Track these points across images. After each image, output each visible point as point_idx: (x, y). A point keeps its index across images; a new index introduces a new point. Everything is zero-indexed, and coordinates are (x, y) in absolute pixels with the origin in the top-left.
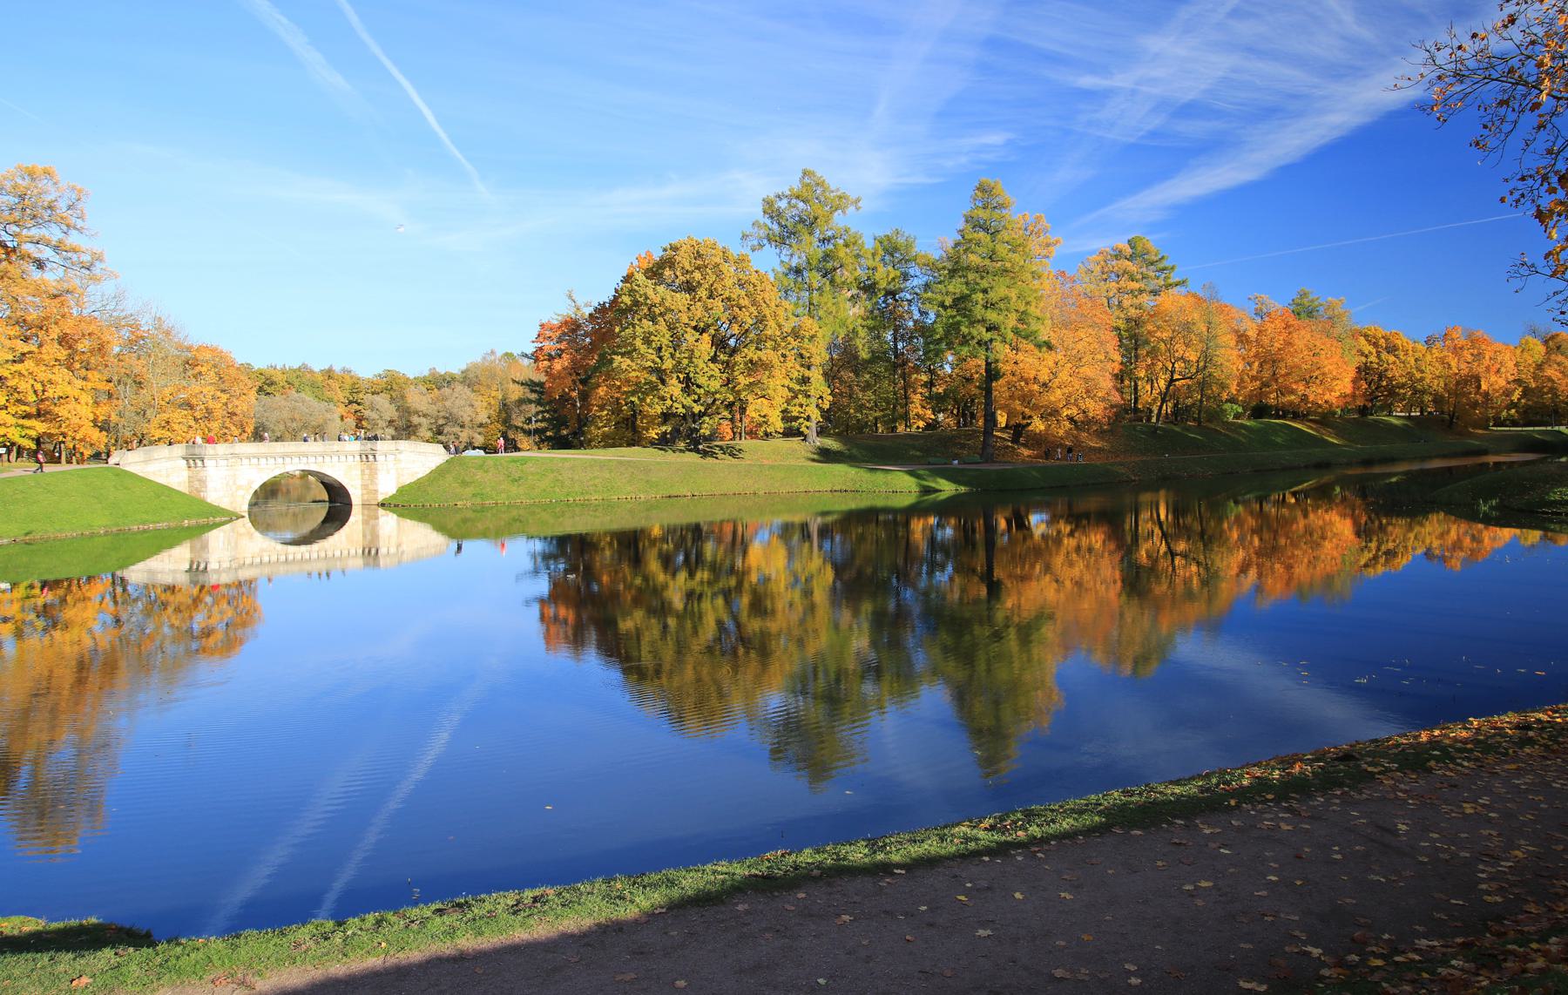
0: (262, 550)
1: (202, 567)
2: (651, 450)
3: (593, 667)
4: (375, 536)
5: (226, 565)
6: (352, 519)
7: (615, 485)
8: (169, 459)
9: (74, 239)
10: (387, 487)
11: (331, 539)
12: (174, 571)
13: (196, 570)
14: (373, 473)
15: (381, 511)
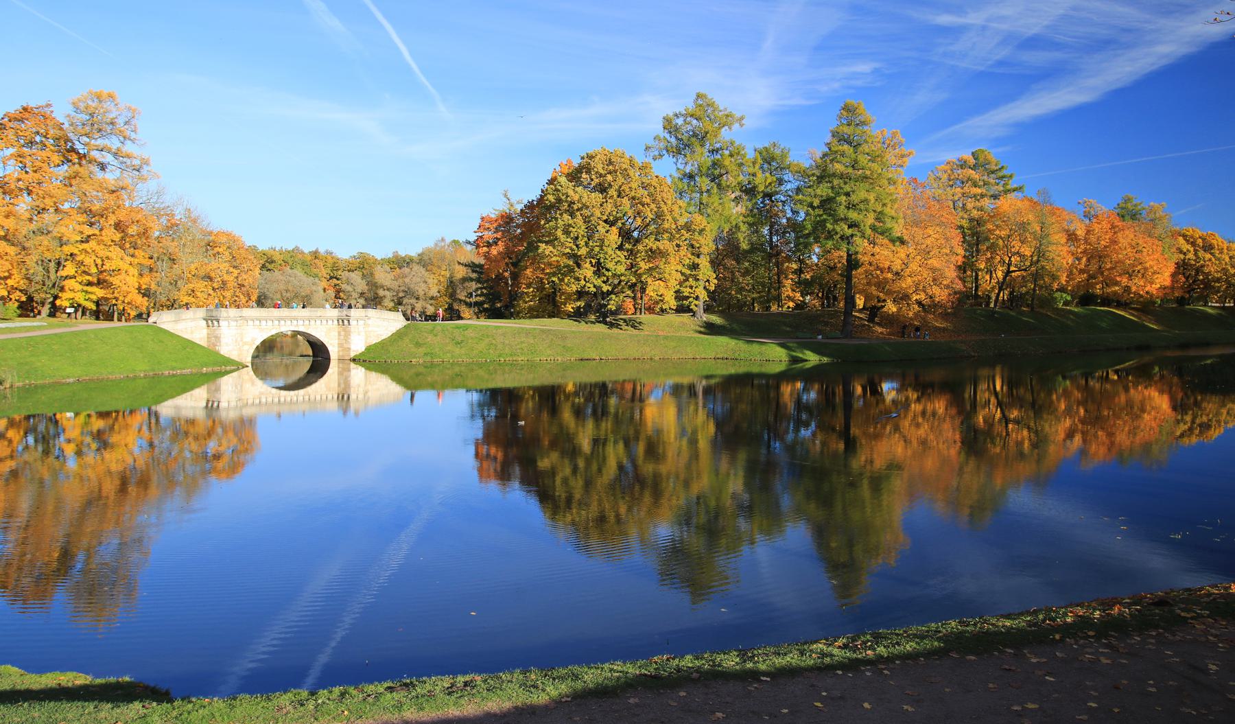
2: (567, 321)
3: (518, 496)
5: (233, 404)
6: (330, 370)
7: (538, 348)
8: (194, 319)
9: (129, 148)
10: (358, 346)
11: (314, 386)
12: (195, 408)
13: (211, 408)
14: (347, 334)
15: (352, 365)
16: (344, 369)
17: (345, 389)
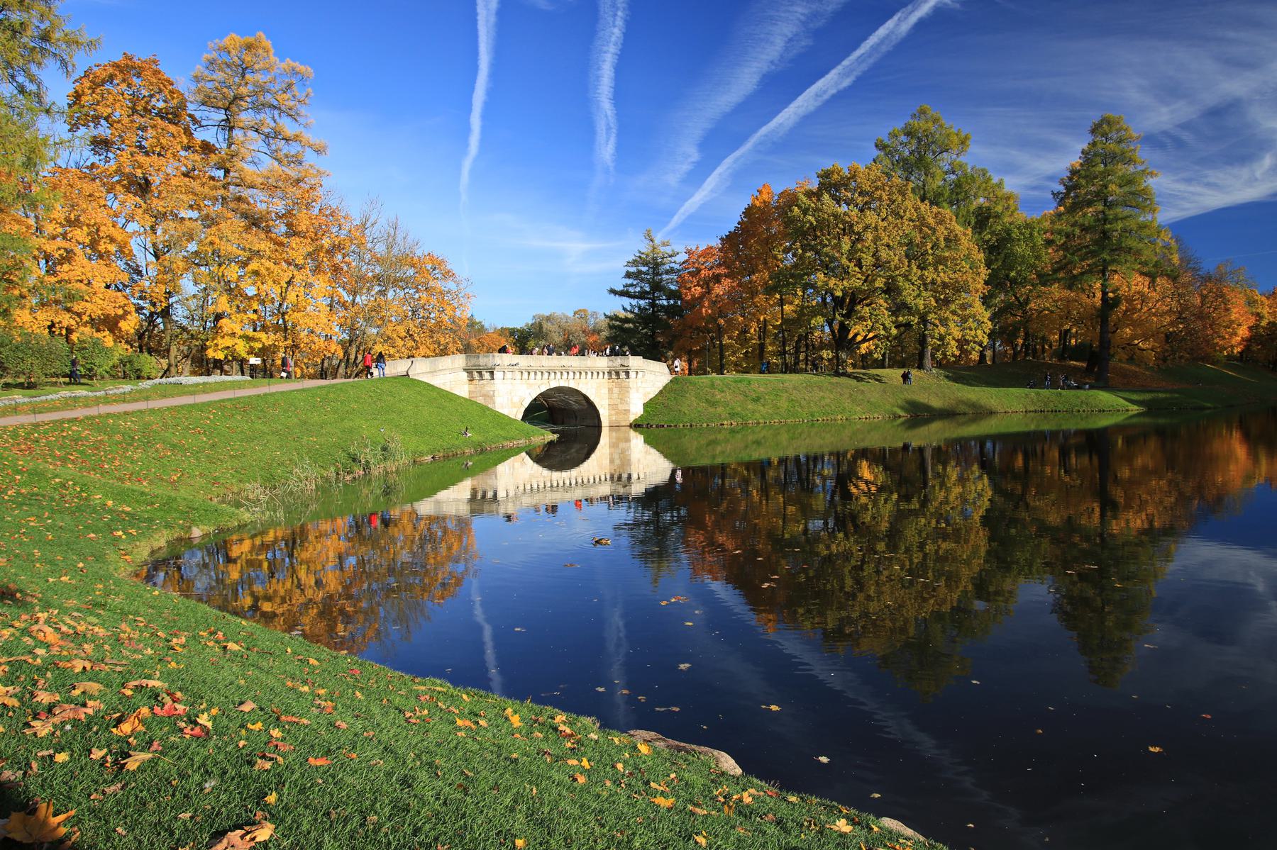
0: (531, 476)
1: (490, 495)
4: (625, 461)
5: (511, 494)
8: (452, 370)
11: (585, 464)
13: (481, 502)
14: (624, 391)
15: (632, 433)
16: (619, 439)
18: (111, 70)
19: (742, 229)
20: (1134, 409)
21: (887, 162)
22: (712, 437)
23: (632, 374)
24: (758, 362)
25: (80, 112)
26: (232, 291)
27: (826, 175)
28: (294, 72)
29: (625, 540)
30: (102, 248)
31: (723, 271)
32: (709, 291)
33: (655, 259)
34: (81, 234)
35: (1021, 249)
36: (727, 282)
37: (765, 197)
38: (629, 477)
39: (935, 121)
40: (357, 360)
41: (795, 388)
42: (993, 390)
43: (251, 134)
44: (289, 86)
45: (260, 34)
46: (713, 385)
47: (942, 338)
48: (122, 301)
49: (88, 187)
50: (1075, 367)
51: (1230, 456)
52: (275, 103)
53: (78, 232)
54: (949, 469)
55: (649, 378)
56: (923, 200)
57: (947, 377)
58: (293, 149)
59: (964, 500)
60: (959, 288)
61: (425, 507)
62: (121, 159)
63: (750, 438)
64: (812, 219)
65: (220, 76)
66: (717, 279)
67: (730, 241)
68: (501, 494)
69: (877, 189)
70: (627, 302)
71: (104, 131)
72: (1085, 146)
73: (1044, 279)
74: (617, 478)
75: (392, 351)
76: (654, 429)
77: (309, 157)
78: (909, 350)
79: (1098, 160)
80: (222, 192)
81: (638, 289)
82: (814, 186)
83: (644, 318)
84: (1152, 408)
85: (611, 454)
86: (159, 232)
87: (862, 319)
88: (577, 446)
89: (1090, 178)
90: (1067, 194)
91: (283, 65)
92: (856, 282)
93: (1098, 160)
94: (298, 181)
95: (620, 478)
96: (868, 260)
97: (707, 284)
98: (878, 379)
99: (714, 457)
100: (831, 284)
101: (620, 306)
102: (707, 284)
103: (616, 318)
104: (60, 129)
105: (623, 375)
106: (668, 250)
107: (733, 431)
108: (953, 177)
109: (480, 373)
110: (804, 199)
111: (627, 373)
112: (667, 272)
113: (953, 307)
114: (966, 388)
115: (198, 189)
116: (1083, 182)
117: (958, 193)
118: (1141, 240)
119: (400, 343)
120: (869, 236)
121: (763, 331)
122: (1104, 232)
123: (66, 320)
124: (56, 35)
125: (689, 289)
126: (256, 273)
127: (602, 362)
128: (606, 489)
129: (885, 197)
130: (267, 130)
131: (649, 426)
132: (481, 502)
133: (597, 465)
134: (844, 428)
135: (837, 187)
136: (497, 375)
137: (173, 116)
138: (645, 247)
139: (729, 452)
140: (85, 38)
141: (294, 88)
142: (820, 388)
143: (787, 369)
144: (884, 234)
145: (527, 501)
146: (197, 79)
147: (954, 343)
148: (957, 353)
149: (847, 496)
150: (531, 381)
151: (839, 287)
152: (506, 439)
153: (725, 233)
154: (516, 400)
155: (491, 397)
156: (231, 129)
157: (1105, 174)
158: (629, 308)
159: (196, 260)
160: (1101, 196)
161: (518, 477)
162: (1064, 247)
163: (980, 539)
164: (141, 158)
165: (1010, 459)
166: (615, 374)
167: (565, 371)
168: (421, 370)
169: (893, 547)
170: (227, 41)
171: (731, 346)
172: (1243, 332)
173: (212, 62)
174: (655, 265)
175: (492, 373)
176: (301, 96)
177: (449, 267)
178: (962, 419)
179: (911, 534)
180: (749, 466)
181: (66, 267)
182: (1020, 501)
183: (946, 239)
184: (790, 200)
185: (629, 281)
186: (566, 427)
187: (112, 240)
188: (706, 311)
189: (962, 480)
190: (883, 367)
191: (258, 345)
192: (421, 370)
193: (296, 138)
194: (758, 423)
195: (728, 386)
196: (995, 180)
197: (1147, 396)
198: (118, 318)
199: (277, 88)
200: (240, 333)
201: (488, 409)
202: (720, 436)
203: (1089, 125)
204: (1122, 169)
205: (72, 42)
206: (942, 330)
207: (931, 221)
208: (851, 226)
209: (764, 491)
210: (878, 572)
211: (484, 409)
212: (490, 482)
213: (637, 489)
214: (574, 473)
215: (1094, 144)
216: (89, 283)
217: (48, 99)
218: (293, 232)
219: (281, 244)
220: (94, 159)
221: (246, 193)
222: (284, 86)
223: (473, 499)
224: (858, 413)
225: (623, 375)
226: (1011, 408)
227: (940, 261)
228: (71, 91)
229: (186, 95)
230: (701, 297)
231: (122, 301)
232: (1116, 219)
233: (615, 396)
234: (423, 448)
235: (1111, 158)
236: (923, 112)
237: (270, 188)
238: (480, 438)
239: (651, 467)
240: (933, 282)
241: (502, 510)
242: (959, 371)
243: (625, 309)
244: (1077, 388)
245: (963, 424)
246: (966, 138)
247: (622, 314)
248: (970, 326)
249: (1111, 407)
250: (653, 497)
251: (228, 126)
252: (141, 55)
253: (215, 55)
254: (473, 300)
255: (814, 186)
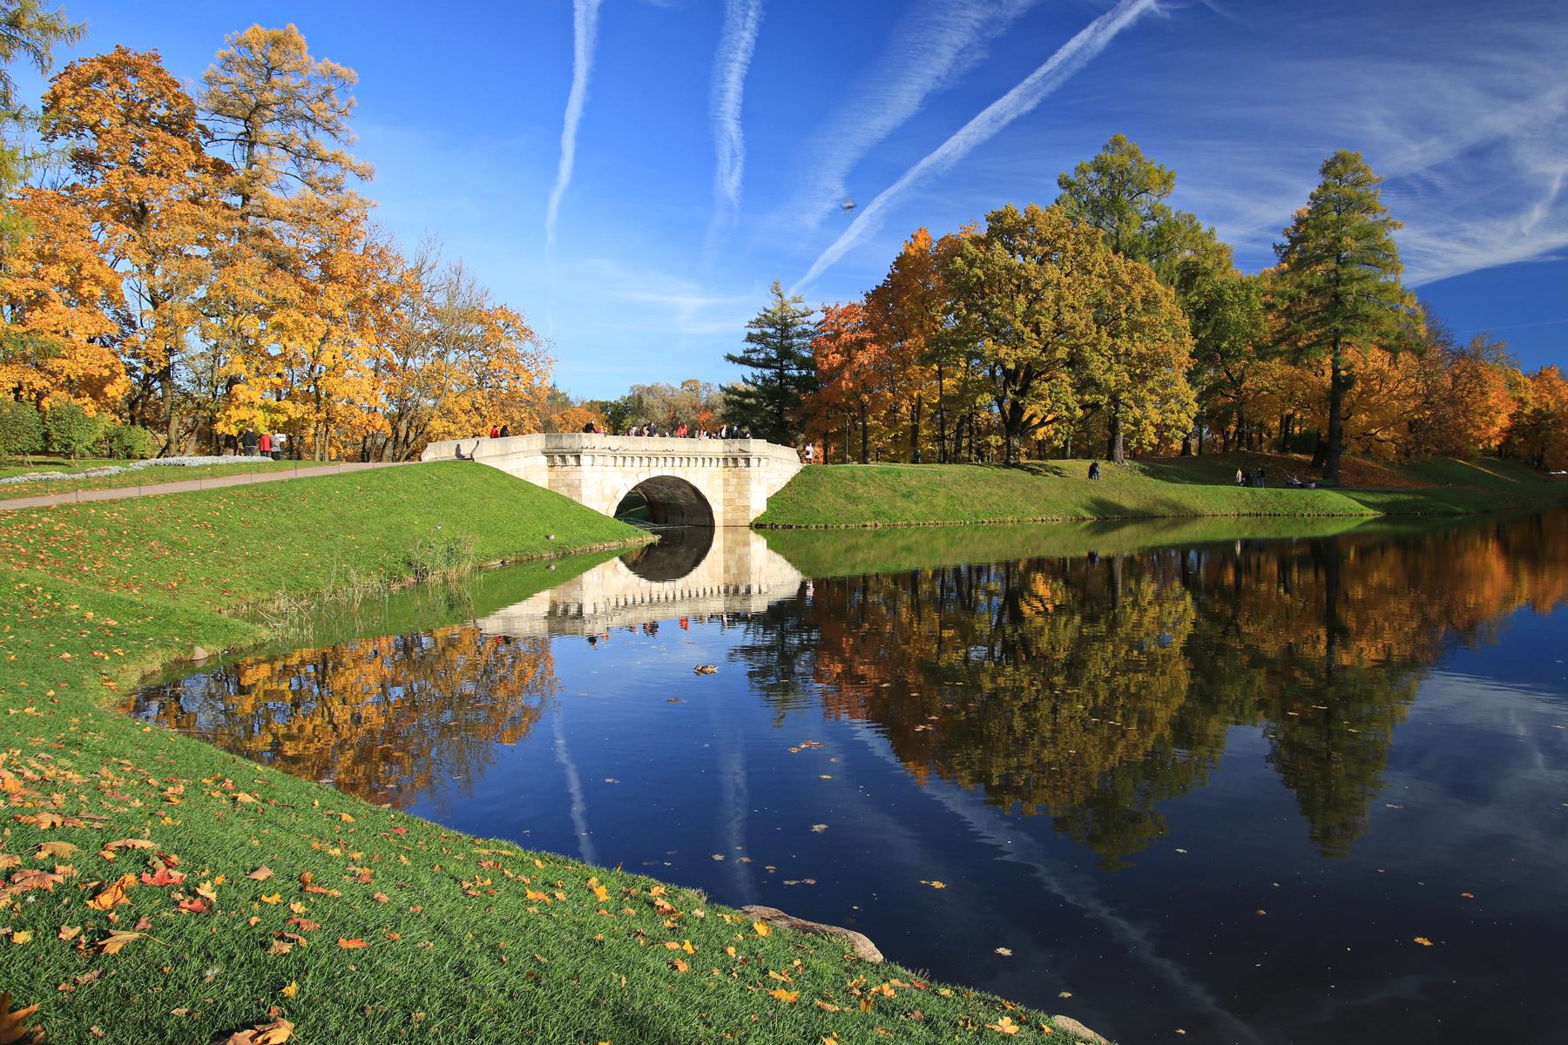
0: (626, 587)
1: (573, 610)
4: (743, 569)
5: (601, 608)
8: (528, 453)
9: (325, 144)
10: (758, 507)
11: (694, 574)
12: (532, 618)
13: (562, 618)
14: (743, 485)
15: (753, 535)
16: (736, 543)
17: (740, 574)
18: (99, 67)
19: (893, 283)
20: (1371, 514)
21: (1073, 203)
22: (851, 541)
23: (754, 462)
24: (909, 449)
25: (58, 116)
26: (250, 349)
27: (997, 218)
28: (334, 75)
29: (742, 666)
30: (85, 290)
31: (867, 335)
32: (851, 360)
33: (782, 318)
34: (57, 272)
35: (1235, 314)
36: (873, 349)
37: (922, 244)
38: (748, 591)
39: (1132, 154)
40: (405, 438)
41: (955, 482)
42: (1199, 488)
43: (278, 152)
44: (327, 92)
45: (293, 27)
46: (854, 477)
47: (1137, 423)
48: (108, 359)
49: (67, 213)
50: (1299, 461)
51: (1484, 574)
52: (309, 114)
53: (53, 270)
54: (1144, 585)
55: (774, 467)
56: (1116, 252)
57: (1142, 471)
58: (331, 171)
59: (1161, 624)
60: (1159, 361)
61: (492, 625)
62: (114, 179)
63: (900, 543)
64: (980, 273)
65: (238, 77)
66: (861, 344)
67: (878, 297)
68: (588, 610)
69: (1060, 236)
70: (748, 371)
71: (89, 143)
72: (1315, 190)
73: (1263, 352)
74: (732, 591)
75: (453, 428)
76: (780, 531)
77: (351, 183)
78: (1097, 437)
79: (1330, 206)
80: (239, 224)
81: (762, 356)
82: (982, 232)
83: (769, 392)
84: (1392, 513)
85: (726, 561)
86: (158, 273)
87: (1040, 397)
88: (682, 550)
89: (1321, 229)
90: (1293, 247)
91: (319, 66)
92: (1032, 352)
93: (1330, 206)
94: (337, 212)
95: (736, 591)
96: (1047, 324)
97: (849, 350)
98: (1057, 472)
99: (854, 566)
100: (1002, 355)
101: (739, 377)
102: (849, 350)
103: (733, 391)
104: (31, 140)
105: (742, 462)
106: (800, 308)
107: (877, 534)
108: (1153, 224)
109: (563, 457)
110: (971, 248)
111: (747, 460)
112: (799, 335)
113: (1150, 384)
114: (1165, 484)
115: (209, 219)
116: (1312, 233)
117: (1159, 244)
118: (1381, 306)
119: (463, 418)
120: (1050, 295)
121: (917, 411)
122: (1336, 296)
123: (39, 383)
124: (28, 20)
125: (826, 356)
126: (280, 326)
127: (717, 446)
128: (718, 605)
129: (1070, 247)
130: (297, 148)
131: (774, 527)
132: (562, 618)
133: (708, 574)
134: (1015, 531)
135: (1010, 233)
136: (585, 459)
137: (178, 125)
138: (772, 304)
139: (872, 560)
140: (66, 23)
141: (333, 95)
142: (986, 482)
143: (945, 458)
144: (1068, 294)
145: (617, 621)
146: (210, 81)
147: (1151, 429)
148: (1156, 441)
149: (1017, 617)
150: (628, 468)
151: (1011, 357)
152: (594, 540)
153: (871, 288)
154: (608, 491)
155: (575, 487)
156: (252, 144)
157: (1339, 224)
158: (750, 379)
159: (207, 308)
160: (1333, 251)
161: (608, 586)
162: (1287, 313)
163: (1180, 670)
164: (137, 180)
165: (1218, 576)
166: (732, 461)
167: (668, 456)
168: (489, 452)
169: (1074, 680)
170: (248, 34)
171: (876, 428)
172: (1503, 421)
173: (229, 60)
174: (784, 326)
175: (578, 457)
176: (342, 105)
177: (525, 324)
178: (1161, 523)
179: (1098, 664)
180: (897, 578)
181: (38, 313)
182: (1230, 626)
183: (1144, 301)
184: (952, 248)
185: (751, 346)
186: (669, 526)
187: (98, 282)
188: (846, 384)
189: (1159, 598)
190: (1065, 457)
191: (282, 419)
192: (489, 452)
193: (335, 159)
194: (909, 525)
195: (872, 478)
196: (1204, 229)
197: (1386, 498)
198: (104, 381)
199: (312, 94)
200: (259, 402)
201: (573, 502)
202: (862, 541)
203: (1320, 163)
204: (1360, 219)
205: (47, 29)
206: (1138, 412)
207: (1126, 278)
208: (1028, 281)
209: (916, 608)
210: (1054, 710)
211: (567, 502)
212: (575, 594)
213: (758, 605)
214: (680, 583)
215: (1325, 187)
216: (67, 335)
217: (16, 101)
218: (329, 276)
219: (314, 291)
220: (77, 179)
221: (271, 226)
222: (320, 92)
223: (552, 613)
224: (1033, 513)
225: (742, 462)
226: (1222, 510)
227: (1135, 327)
228: (48, 92)
229: (195, 100)
230: (842, 366)
231: (108, 359)
232: (1351, 279)
233: (732, 488)
234: (490, 550)
235: (1346, 205)
236: (1117, 143)
237: (302, 221)
238: (563, 539)
239: (775, 577)
240: (1127, 354)
241: (588, 628)
242: (1157, 464)
243: (745, 380)
244: (1302, 486)
245: (1163, 528)
246: (1170, 176)
247: (742, 386)
248: (1171, 408)
249: (1341, 511)
250: (778, 614)
251: (248, 140)
252: (138, 48)
253: (232, 51)
254: (554, 365)
255: (982, 232)
